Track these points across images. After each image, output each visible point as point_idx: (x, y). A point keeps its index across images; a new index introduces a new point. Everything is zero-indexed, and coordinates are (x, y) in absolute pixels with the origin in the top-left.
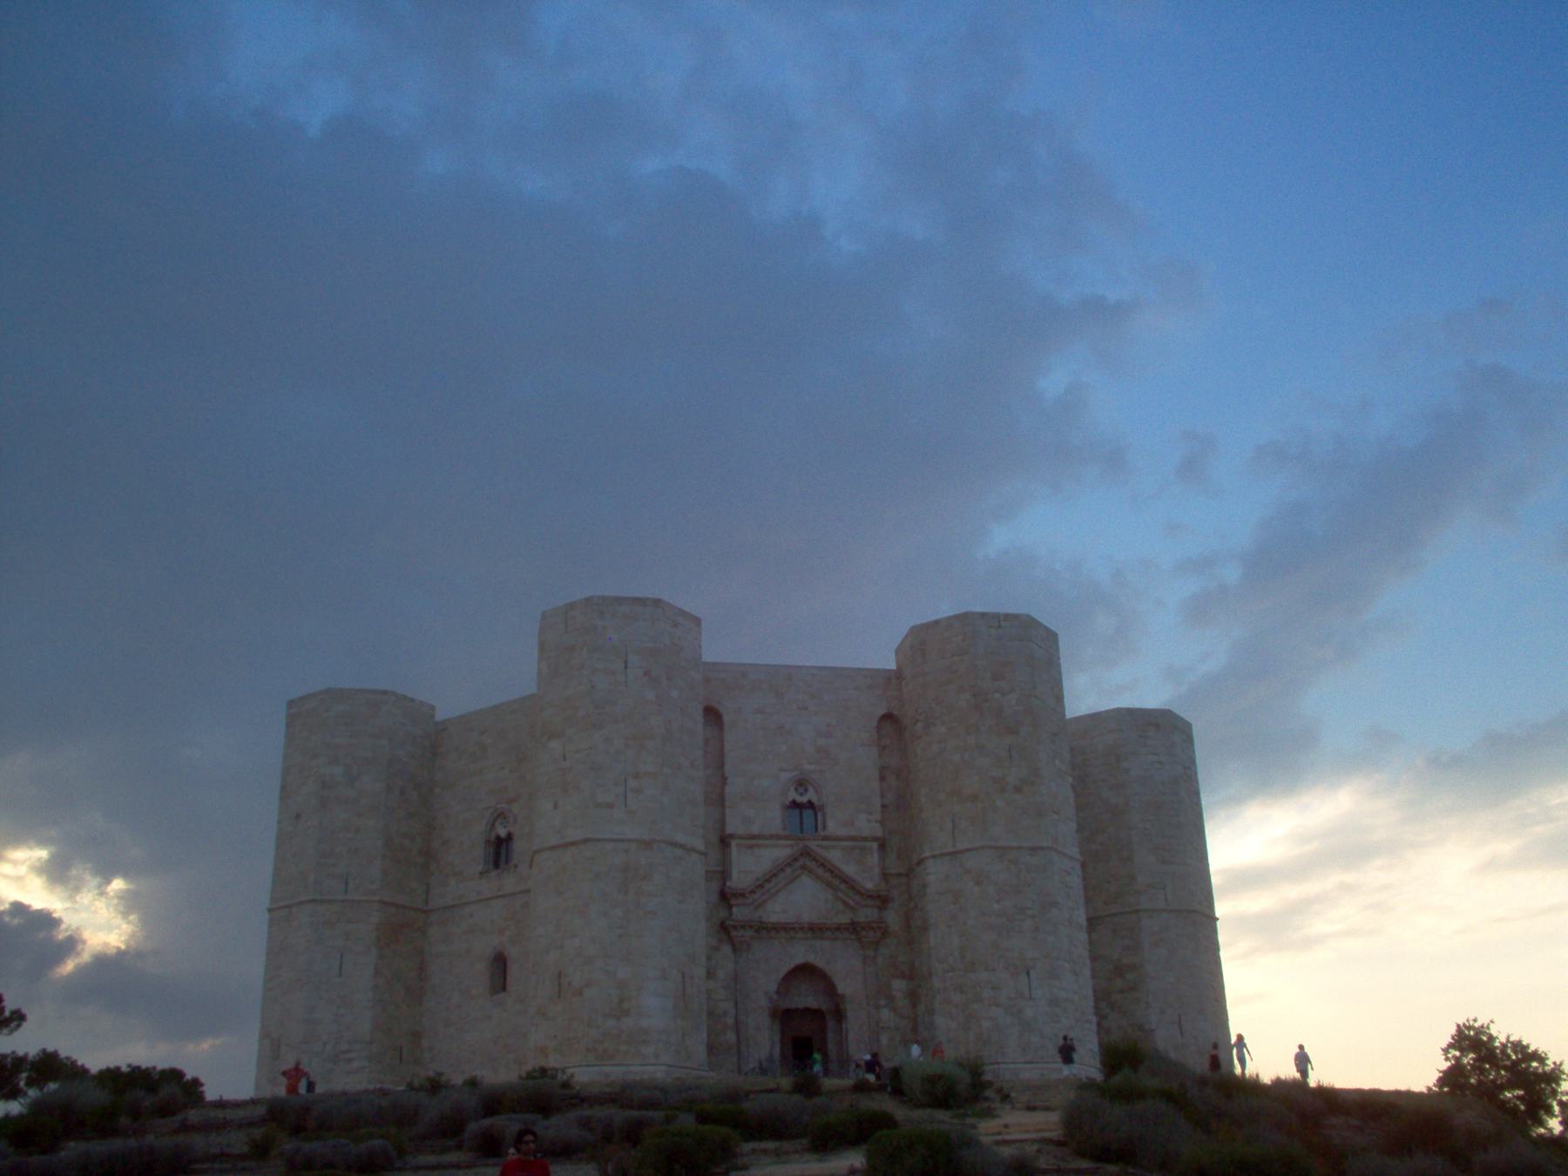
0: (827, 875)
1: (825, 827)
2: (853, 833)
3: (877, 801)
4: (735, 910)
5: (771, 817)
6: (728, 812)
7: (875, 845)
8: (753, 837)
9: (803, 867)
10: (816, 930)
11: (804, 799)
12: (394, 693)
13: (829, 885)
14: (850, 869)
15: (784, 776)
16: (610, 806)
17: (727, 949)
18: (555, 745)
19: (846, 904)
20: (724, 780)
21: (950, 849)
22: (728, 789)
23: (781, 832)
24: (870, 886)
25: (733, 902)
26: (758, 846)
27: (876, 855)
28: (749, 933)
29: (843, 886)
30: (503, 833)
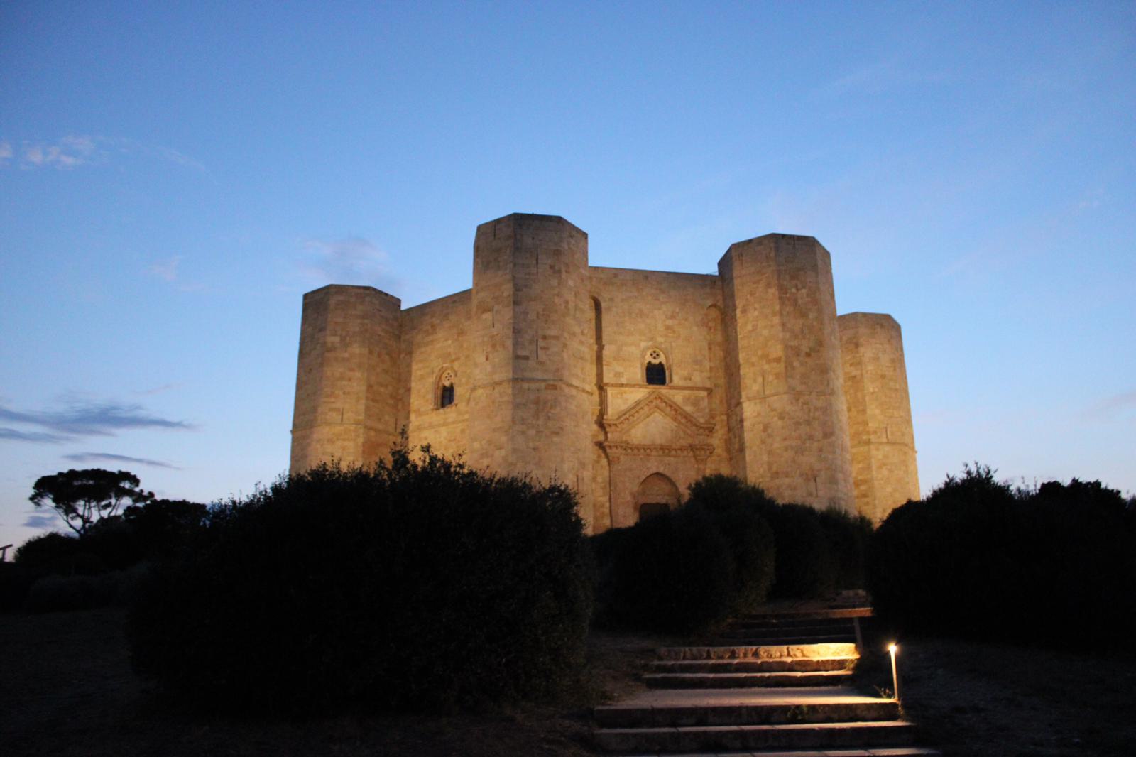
0: (673, 413)
1: (671, 380)
2: (689, 384)
3: (707, 364)
4: (609, 435)
5: (639, 374)
6: (605, 368)
7: (704, 394)
8: (622, 385)
9: (657, 407)
10: (665, 450)
11: (656, 362)
12: (374, 289)
13: (675, 419)
14: (688, 409)
15: (643, 344)
16: (526, 358)
17: (604, 462)
18: (487, 316)
19: (685, 432)
20: (601, 347)
21: (763, 396)
22: (605, 352)
23: (641, 383)
24: (702, 420)
25: (607, 430)
26: (625, 393)
27: (706, 401)
28: (619, 450)
29: (684, 421)
30: (447, 384)
